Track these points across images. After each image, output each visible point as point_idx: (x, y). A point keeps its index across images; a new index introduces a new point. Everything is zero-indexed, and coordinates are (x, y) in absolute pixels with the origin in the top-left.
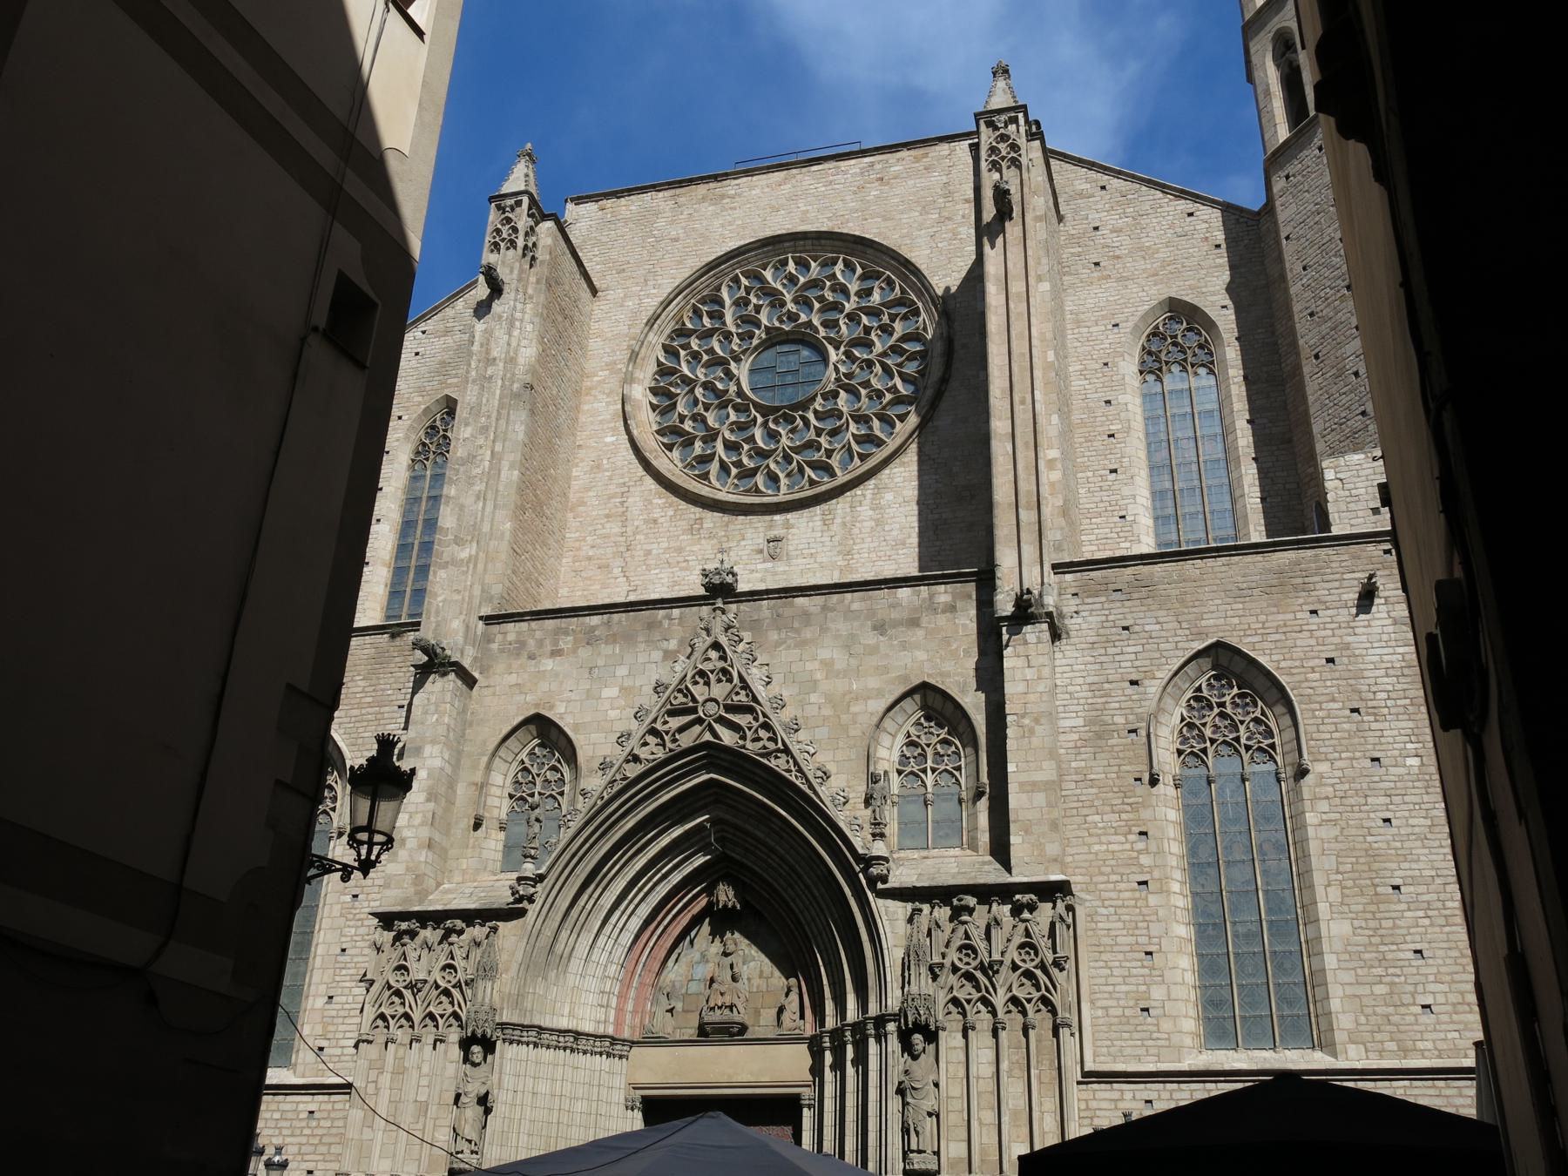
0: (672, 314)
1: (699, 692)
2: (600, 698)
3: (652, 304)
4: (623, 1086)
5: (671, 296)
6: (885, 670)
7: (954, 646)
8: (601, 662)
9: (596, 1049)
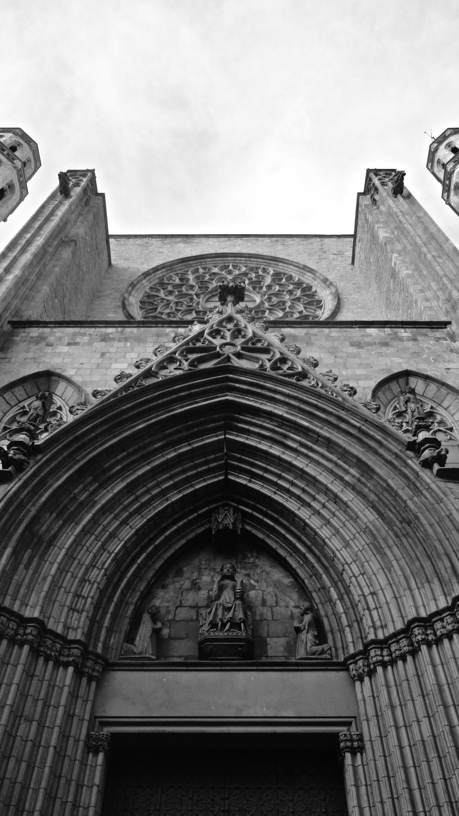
0: (158, 276)
1: (217, 342)
2: (110, 368)
3: (146, 267)
4: (87, 717)
5: (159, 267)
6: (368, 366)
7: (425, 356)
8: (112, 350)
9: (62, 658)
